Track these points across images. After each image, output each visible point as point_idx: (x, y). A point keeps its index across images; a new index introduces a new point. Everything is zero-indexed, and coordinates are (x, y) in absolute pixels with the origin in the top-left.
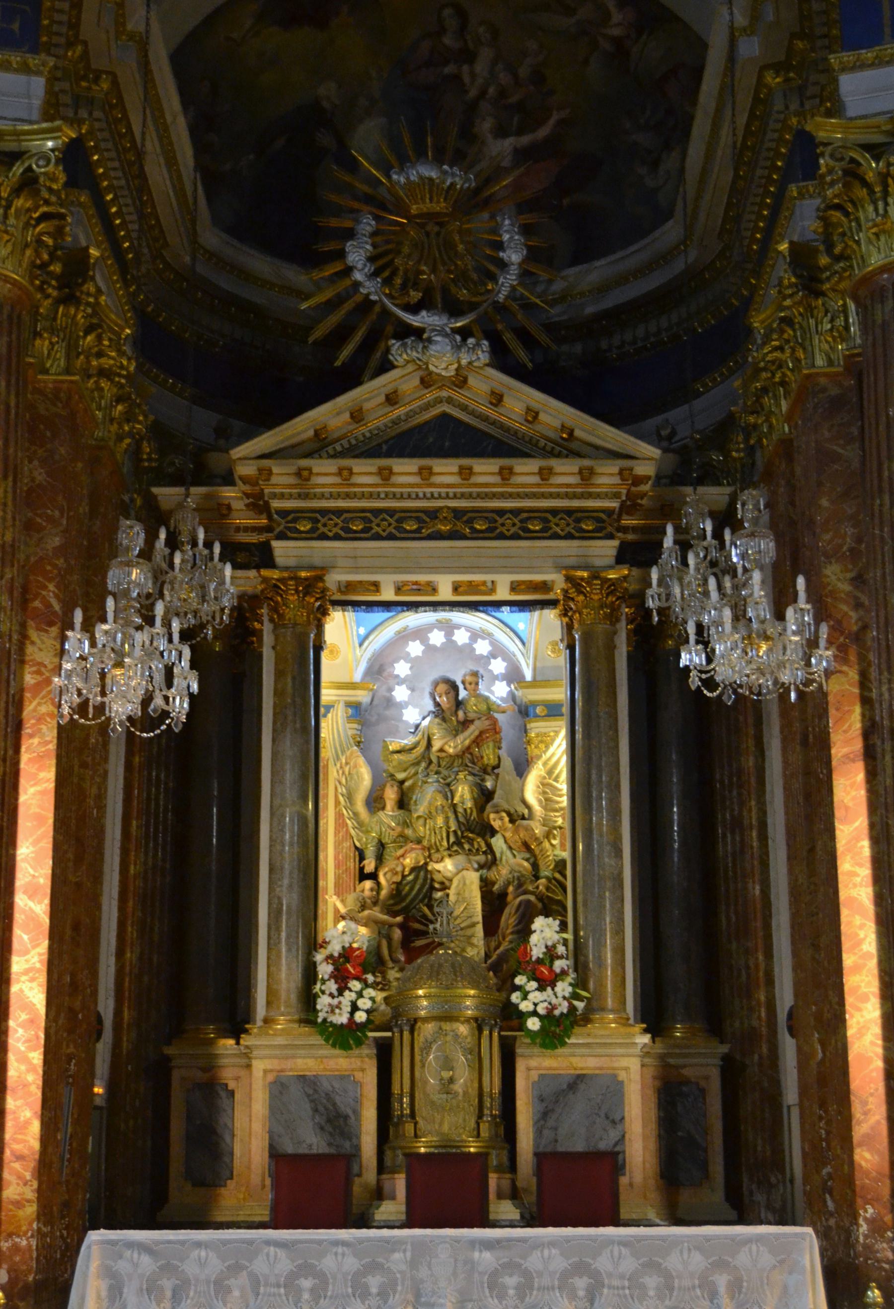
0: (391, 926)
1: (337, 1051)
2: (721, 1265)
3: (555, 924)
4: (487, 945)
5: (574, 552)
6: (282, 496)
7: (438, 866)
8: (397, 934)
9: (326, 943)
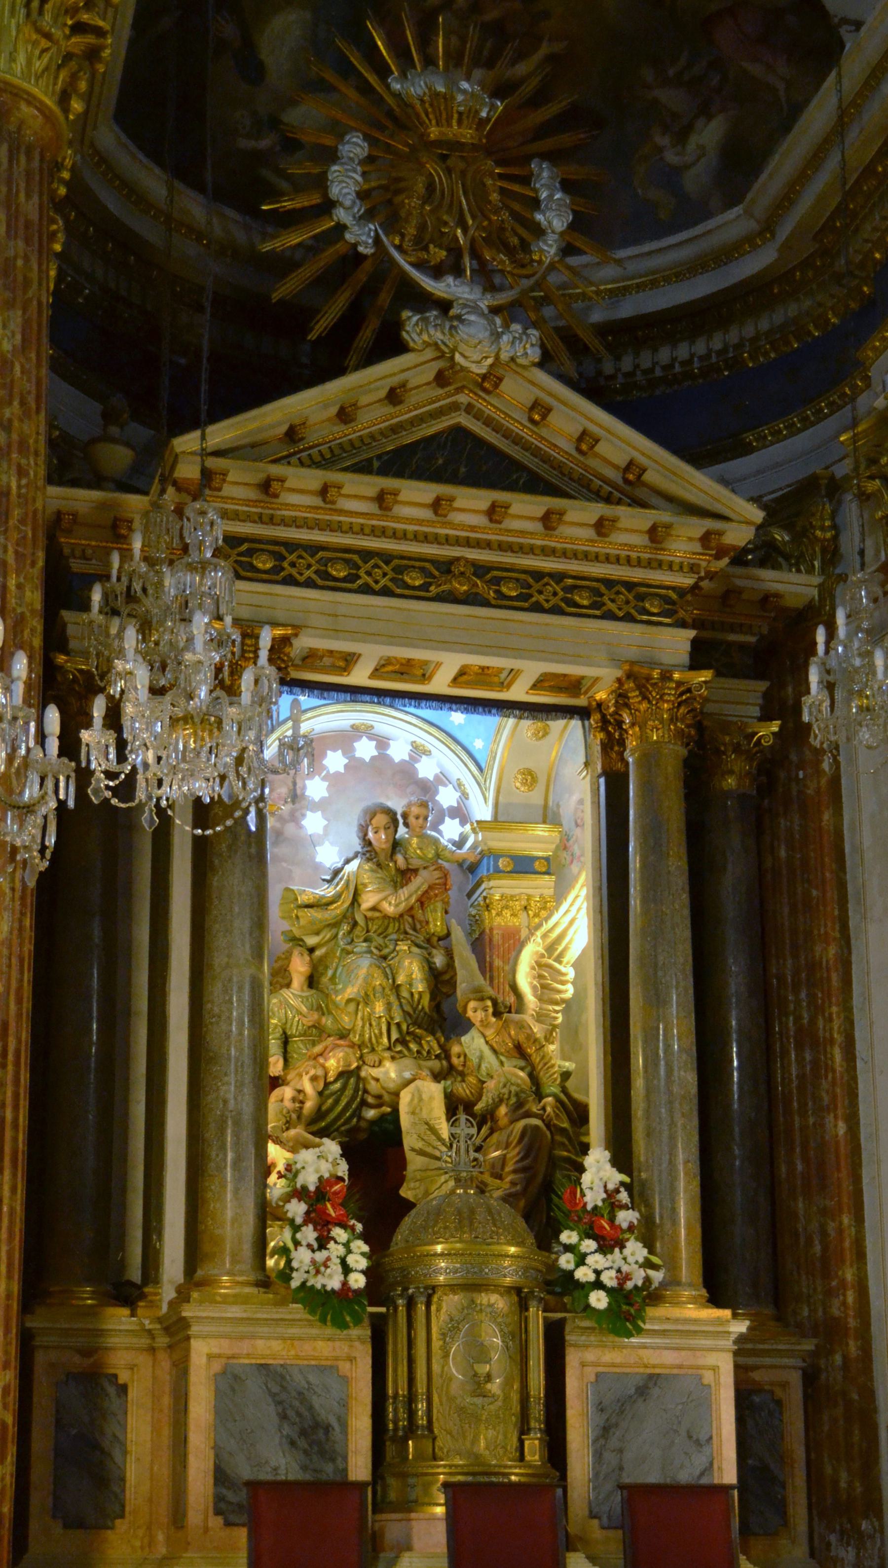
1: (330, 1331)
7: (375, 1072)
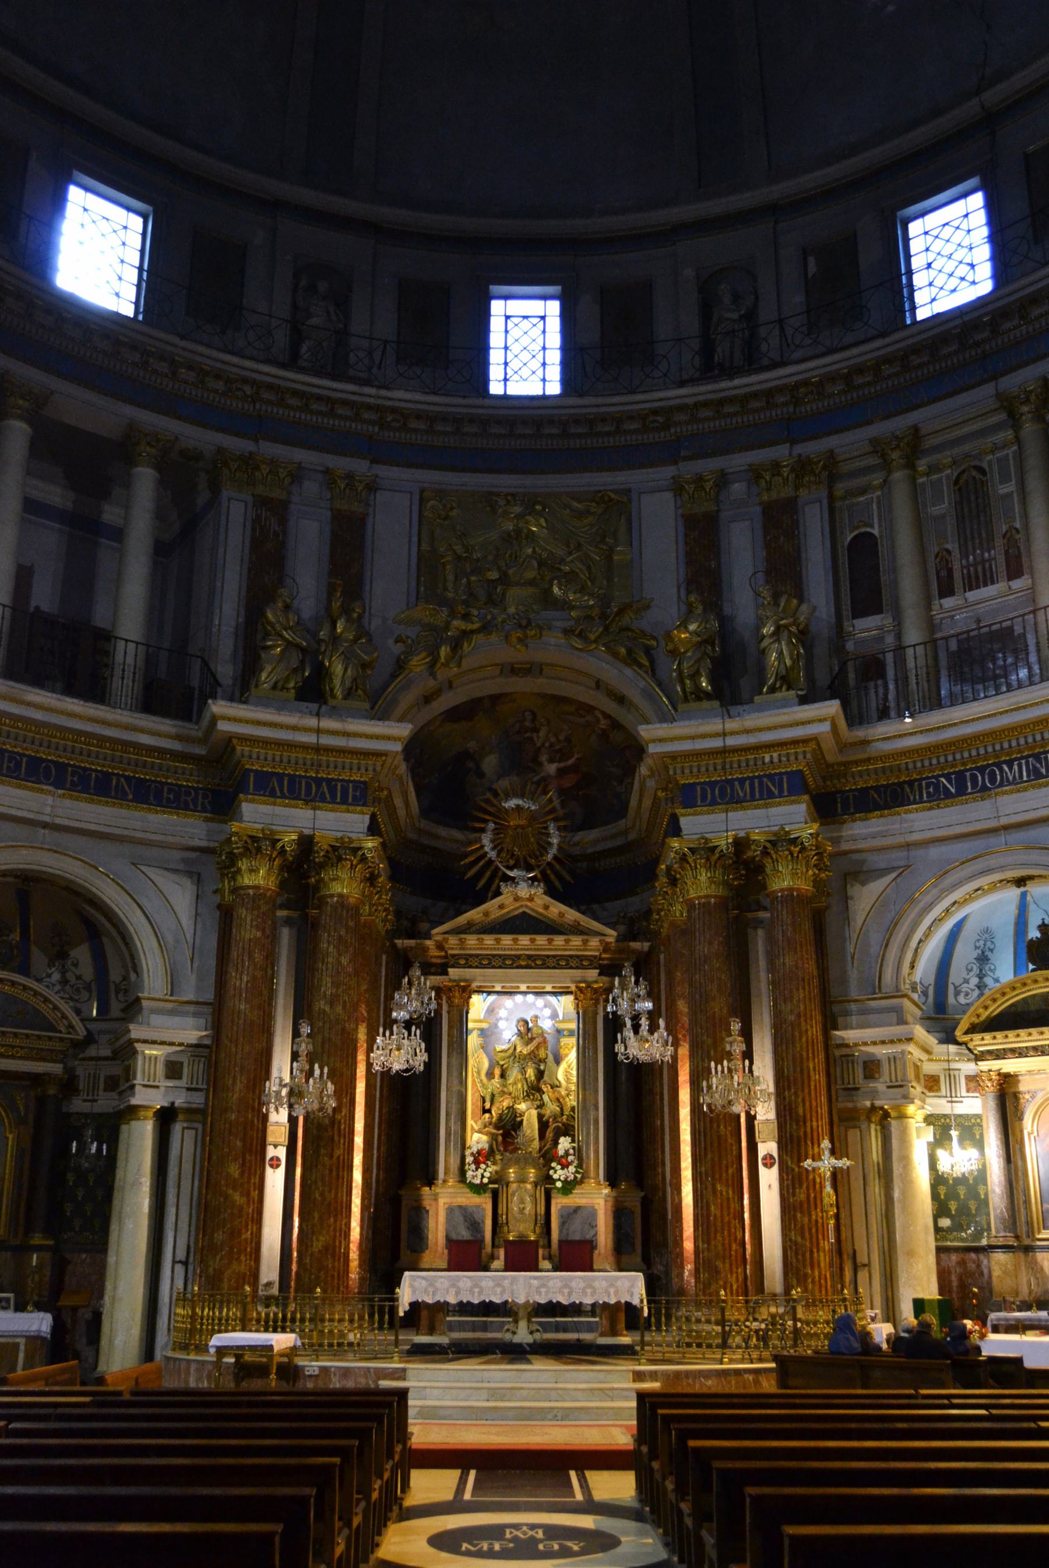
2: (612, 1285)
3: (569, 1139)
6: (452, 949)
8: (500, 1138)
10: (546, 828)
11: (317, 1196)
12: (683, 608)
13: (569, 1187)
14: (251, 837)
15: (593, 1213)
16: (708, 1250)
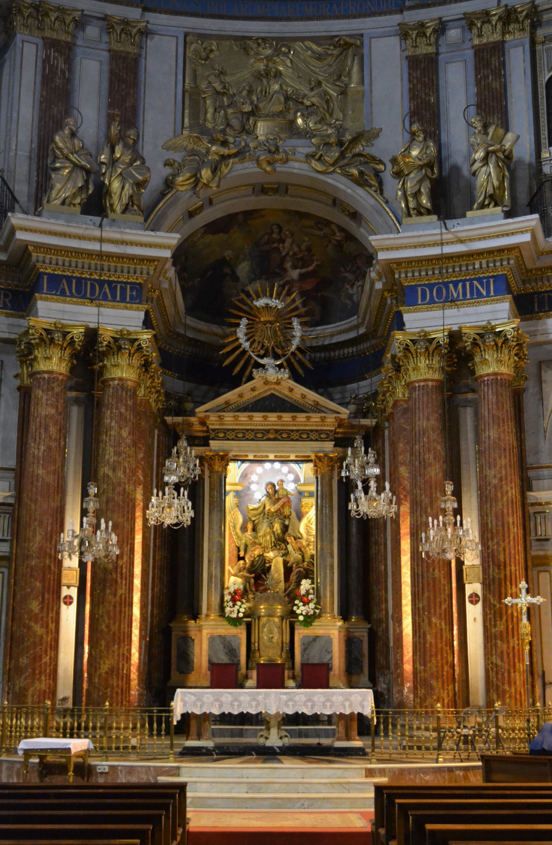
0: (250, 578)
1: (232, 627)
2: (347, 700)
4: (285, 585)
5: (319, 446)
6: (213, 424)
8: (252, 581)
9: (228, 588)
10: (291, 323)
11: (103, 627)
12: (408, 136)
13: (309, 620)
14: (45, 330)
15: (329, 641)
16: (425, 671)
